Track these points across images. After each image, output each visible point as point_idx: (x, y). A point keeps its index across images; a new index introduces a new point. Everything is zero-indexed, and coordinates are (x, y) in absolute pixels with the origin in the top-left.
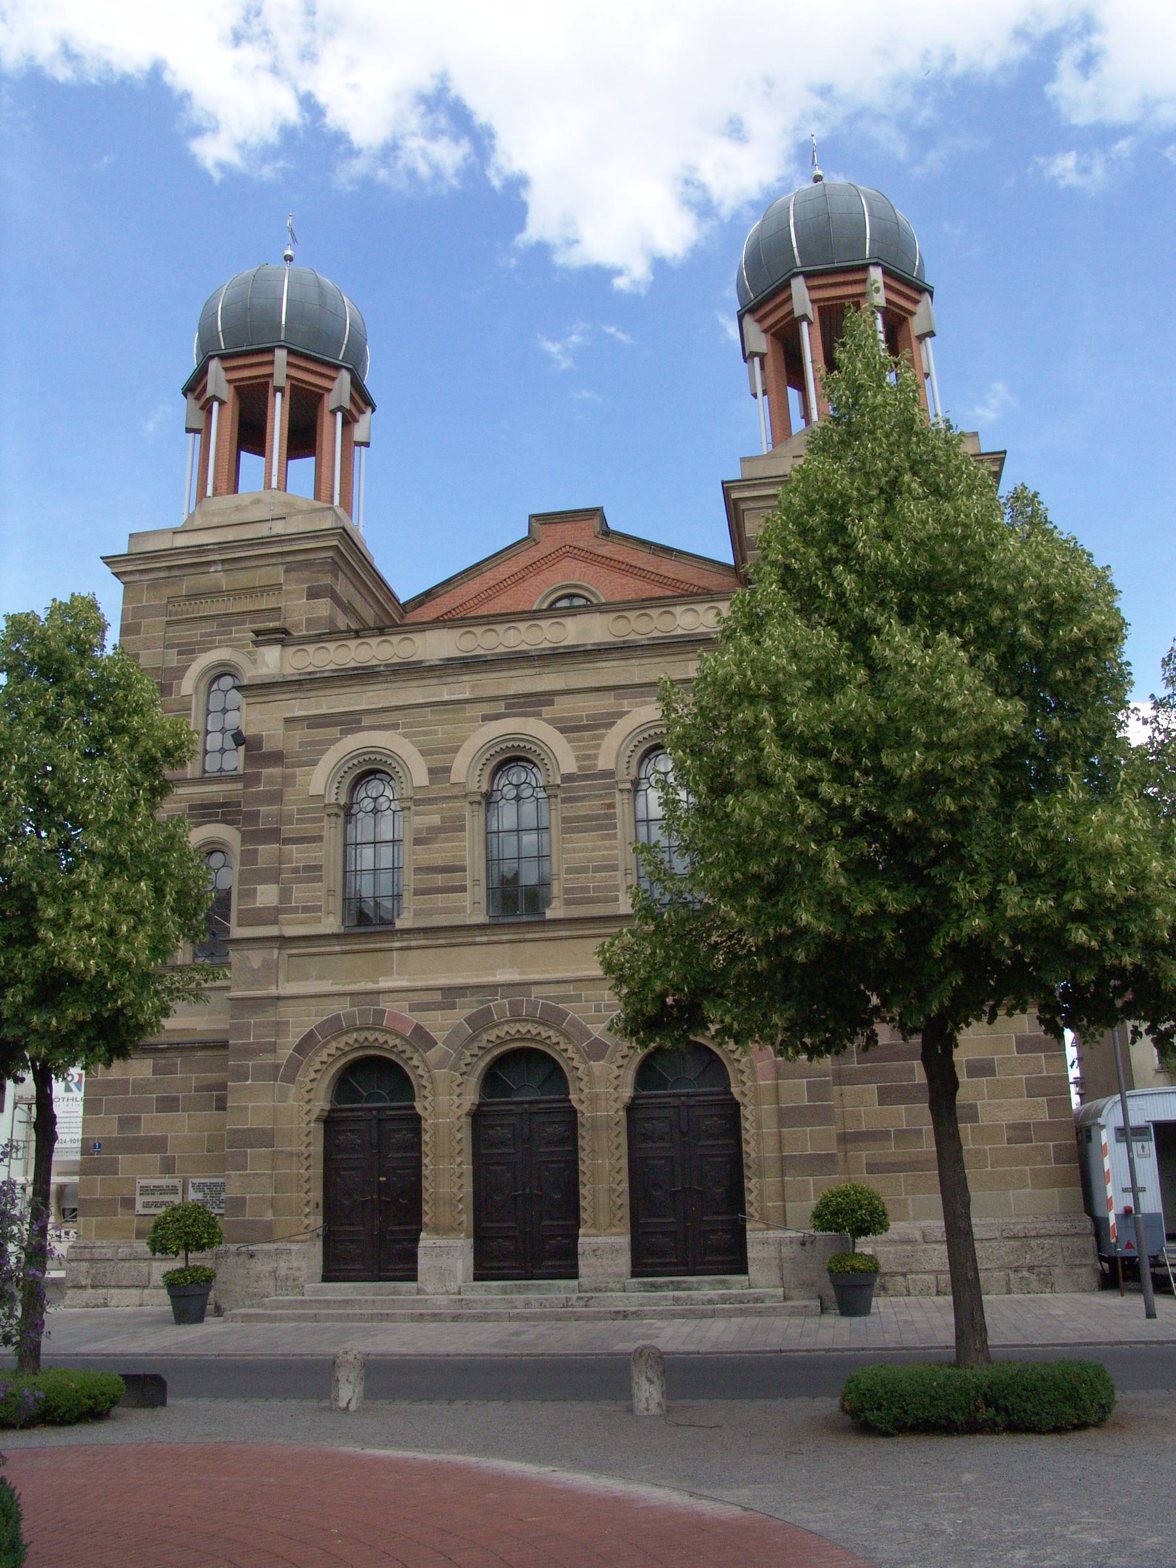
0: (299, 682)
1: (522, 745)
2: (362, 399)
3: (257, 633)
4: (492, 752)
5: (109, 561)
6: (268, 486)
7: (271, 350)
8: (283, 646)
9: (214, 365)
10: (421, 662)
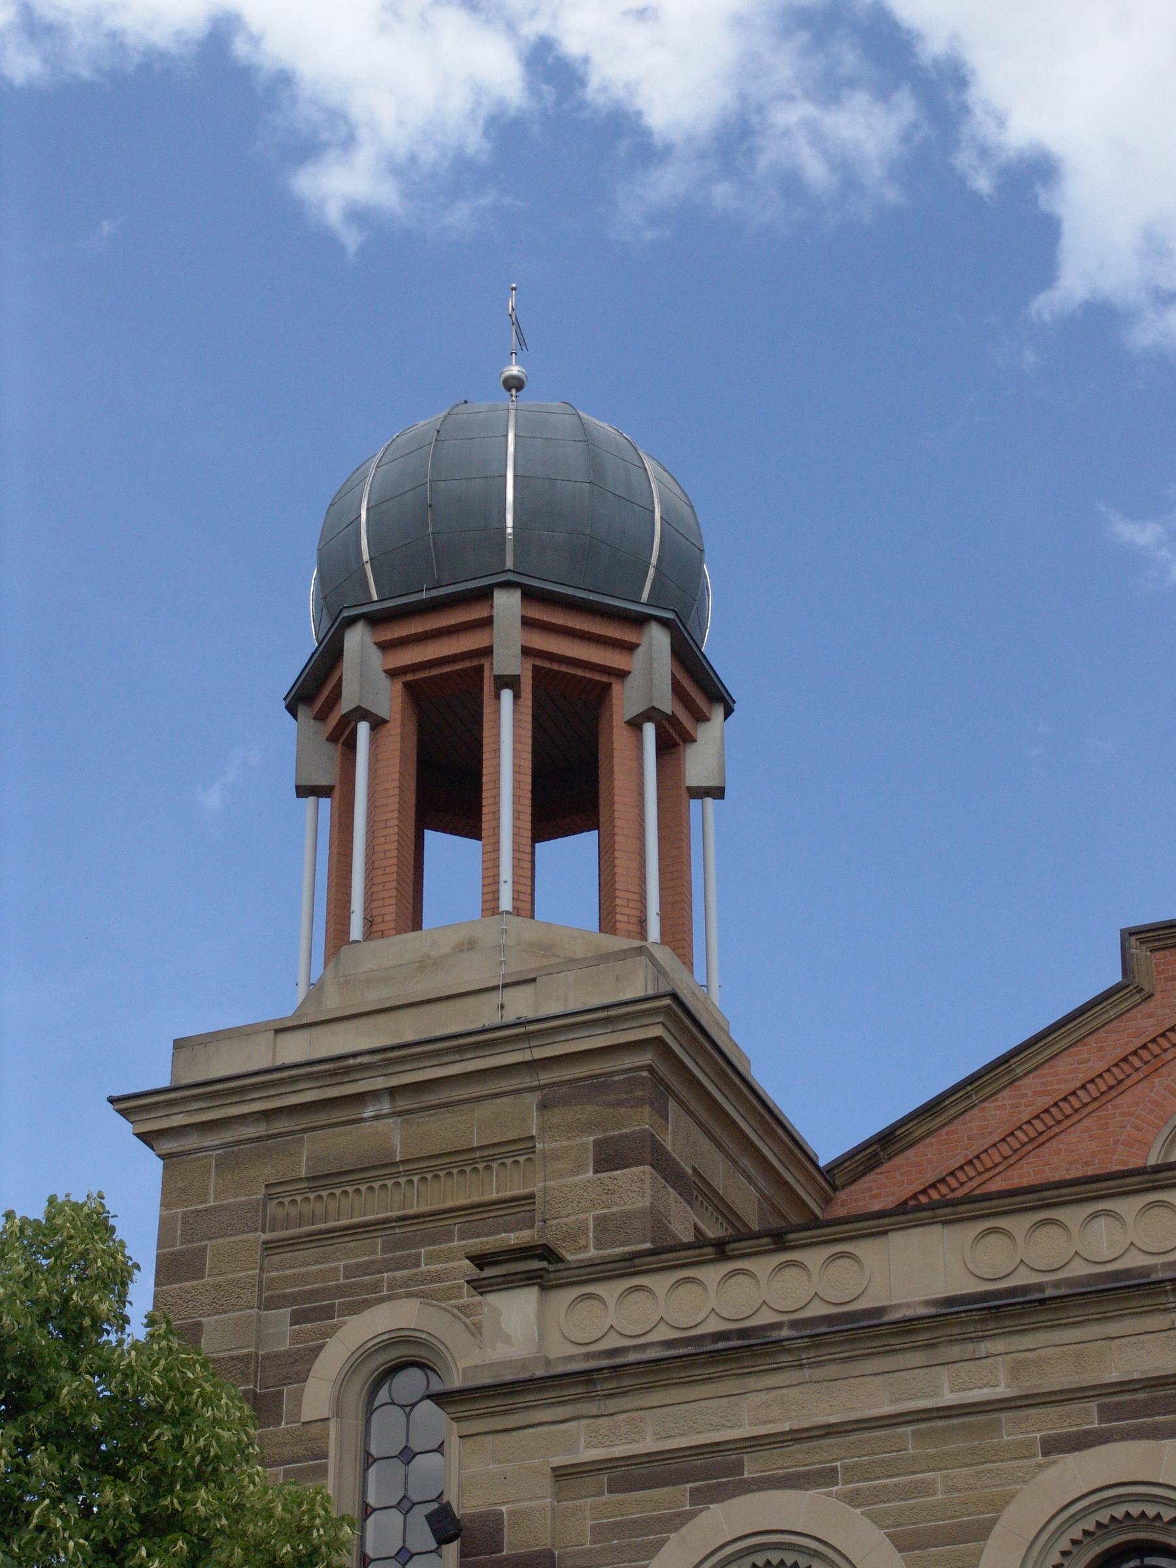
0: (585, 1377)
1: (1151, 1511)
2: (701, 688)
3: (481, 1260)
4: (1076, 1532)
5: (128, 1106)
6: (491, 906)
7: (484, 595)
8: (544, 1288)
9: (357, 639)
10: (880, 1311)
